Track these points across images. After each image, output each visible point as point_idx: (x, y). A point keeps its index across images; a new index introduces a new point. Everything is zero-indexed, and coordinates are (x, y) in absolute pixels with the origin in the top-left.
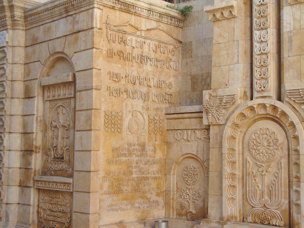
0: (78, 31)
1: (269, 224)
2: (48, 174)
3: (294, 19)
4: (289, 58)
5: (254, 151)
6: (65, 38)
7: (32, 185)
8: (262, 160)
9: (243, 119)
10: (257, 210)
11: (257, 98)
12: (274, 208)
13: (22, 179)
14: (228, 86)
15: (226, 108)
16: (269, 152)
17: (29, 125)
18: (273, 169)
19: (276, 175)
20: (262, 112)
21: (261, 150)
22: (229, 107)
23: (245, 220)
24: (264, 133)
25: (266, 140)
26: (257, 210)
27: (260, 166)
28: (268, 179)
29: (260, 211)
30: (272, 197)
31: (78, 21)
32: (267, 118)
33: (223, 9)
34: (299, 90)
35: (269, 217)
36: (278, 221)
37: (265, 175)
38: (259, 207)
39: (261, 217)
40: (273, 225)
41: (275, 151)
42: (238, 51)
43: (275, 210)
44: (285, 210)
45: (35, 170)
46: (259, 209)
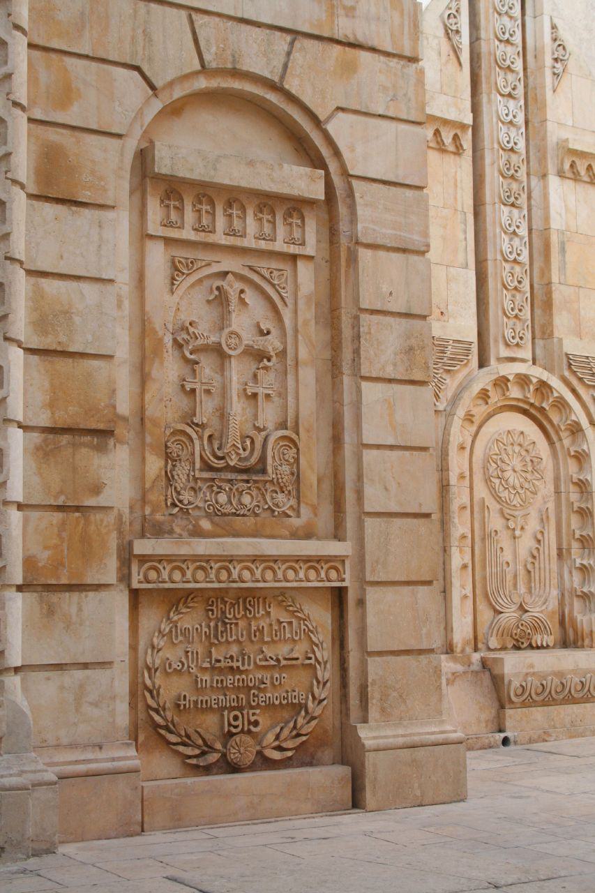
0: (352, 40)
1: (531, 647)
2: (177, 530)
3: (567, 209)
4: (562, 287)
5: (497, 481)
7: (111, 576)
8: (515, 502)
9: (477, 405)
10: (508, 619)
11: (499, 360)
12: (538, 609)
13: (44, 556)
14: (445, 318)
15: (449, 370)
16: (526, 485)
17: (77, 319)
18: (533, 525)
19: (539, 537)
20: (515, 392)
21: (511, 480)
22: (457, 371)
23: (480, 645)
24: (516, 439)
25: (520, 459)
26: (508, 619)
27: (508, 517)
28: (526, 543)
29: (512, 620)
30: (533, 585)
32: (525, 412)
33: (446, 122)
34: (587, 357)
35: (529, 631)
36: (545, 636)
37: (520, 537)
38: (512, 610)
39: (516, 634)
40: (538, 648)
41: (536, 482)
42: (466, 238)
43: (541, 615)
44: (553, 613)
45: (120, 516)
46: (510, 615)
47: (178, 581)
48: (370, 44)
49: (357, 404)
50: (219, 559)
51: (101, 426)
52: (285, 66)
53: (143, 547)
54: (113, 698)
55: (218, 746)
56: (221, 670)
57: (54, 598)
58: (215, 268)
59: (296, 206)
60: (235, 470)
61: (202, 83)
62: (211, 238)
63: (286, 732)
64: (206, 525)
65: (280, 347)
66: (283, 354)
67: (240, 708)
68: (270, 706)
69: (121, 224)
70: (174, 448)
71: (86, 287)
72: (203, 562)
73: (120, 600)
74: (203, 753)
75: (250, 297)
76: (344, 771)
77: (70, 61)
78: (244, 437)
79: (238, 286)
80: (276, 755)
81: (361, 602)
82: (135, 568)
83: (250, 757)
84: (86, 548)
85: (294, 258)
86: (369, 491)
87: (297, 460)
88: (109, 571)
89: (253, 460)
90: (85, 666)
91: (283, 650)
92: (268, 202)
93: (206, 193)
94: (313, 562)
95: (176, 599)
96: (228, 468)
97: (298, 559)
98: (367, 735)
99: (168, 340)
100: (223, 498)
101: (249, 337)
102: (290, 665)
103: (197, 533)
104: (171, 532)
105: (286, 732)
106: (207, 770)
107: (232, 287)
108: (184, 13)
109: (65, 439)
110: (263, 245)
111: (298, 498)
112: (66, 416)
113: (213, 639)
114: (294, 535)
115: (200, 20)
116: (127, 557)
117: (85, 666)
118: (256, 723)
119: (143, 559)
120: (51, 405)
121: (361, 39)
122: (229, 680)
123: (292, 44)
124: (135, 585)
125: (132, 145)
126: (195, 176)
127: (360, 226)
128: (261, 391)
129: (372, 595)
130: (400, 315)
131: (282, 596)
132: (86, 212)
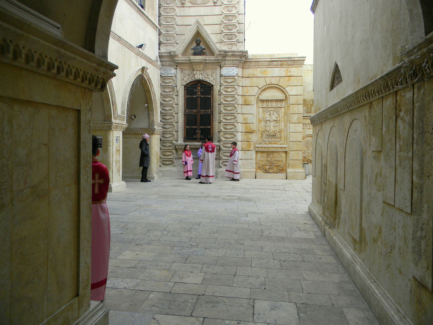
0: (290, 76)
2: (263, 143)
6: (279, 78)
17: (248, 119)
31: (291, 71)
47: (261, 150)
48: (293, 76)
49: (289, 127)
50: (268, 147)
51: (252, 131)
52: (279, 82)
53: (257, 146)
54: (253, 163)
55: (268, 170)
56: (268, 161)
57: (246, 151)
58: (269, 110)
59: (281, 101)
60: (272, 136)
61: (267, 86)
62: (268, 106)
63: (278, 169)
64: (267, 143)
65: (279, 119)
66: (279, 120)
67: (271, 166)
68: (275, 166)
69: (255, 106)
70: (263, 133)
71: (250, 115)
72: (265, 147)
73: (254, 153)
74: (266, 171)
75: (275, 113)
76: (285, 174)
77: (248, 87)
78: (273, 131)
79: (273, 112)
80: (276, 172)
81: (289, 153)
82: (256, 148)
83: (272, 172)
84: (249, 146)
85: (281, 107)
86: (290, 138)
87: (281, 134)
88: (252, 148)
89: (274, 135)
90: (250, 159)
91: (277, 159)
92: (277, 101)
93: (267, 101)
94: (281, 148)
95: (262, 152)
96: (271, 136)
97: (279, 147)
98: (288, 170)
99: (262, 120)
100: (270, 139)
101: (274, 119)
102: (279, 161)
103: (266, 144)
104: (262, 144)
105: (278, 169)
106: (266, 173)
107: (272, 112)
108: (264, 78)
109: (247, 133)
110: (276, 106)
111: (281, 139)
112: (247, 131)
113: (267, 157)
114: (281, 144)
115: (266, 78)
116: (255, 147)
117: (250, 159)
118: (273, 168)
119: (257, 147)
120: (246, 129)
121: (292, 75)
122: (270, 162)
123: (280, 78)
124: (256, 150)
125: (257, 96)
126: (265, 99)
127: (290, 102)
128: (276, 126)
129: (290, 152)
130: (297, 114)
131: (277, 152)
132: (250, 106)
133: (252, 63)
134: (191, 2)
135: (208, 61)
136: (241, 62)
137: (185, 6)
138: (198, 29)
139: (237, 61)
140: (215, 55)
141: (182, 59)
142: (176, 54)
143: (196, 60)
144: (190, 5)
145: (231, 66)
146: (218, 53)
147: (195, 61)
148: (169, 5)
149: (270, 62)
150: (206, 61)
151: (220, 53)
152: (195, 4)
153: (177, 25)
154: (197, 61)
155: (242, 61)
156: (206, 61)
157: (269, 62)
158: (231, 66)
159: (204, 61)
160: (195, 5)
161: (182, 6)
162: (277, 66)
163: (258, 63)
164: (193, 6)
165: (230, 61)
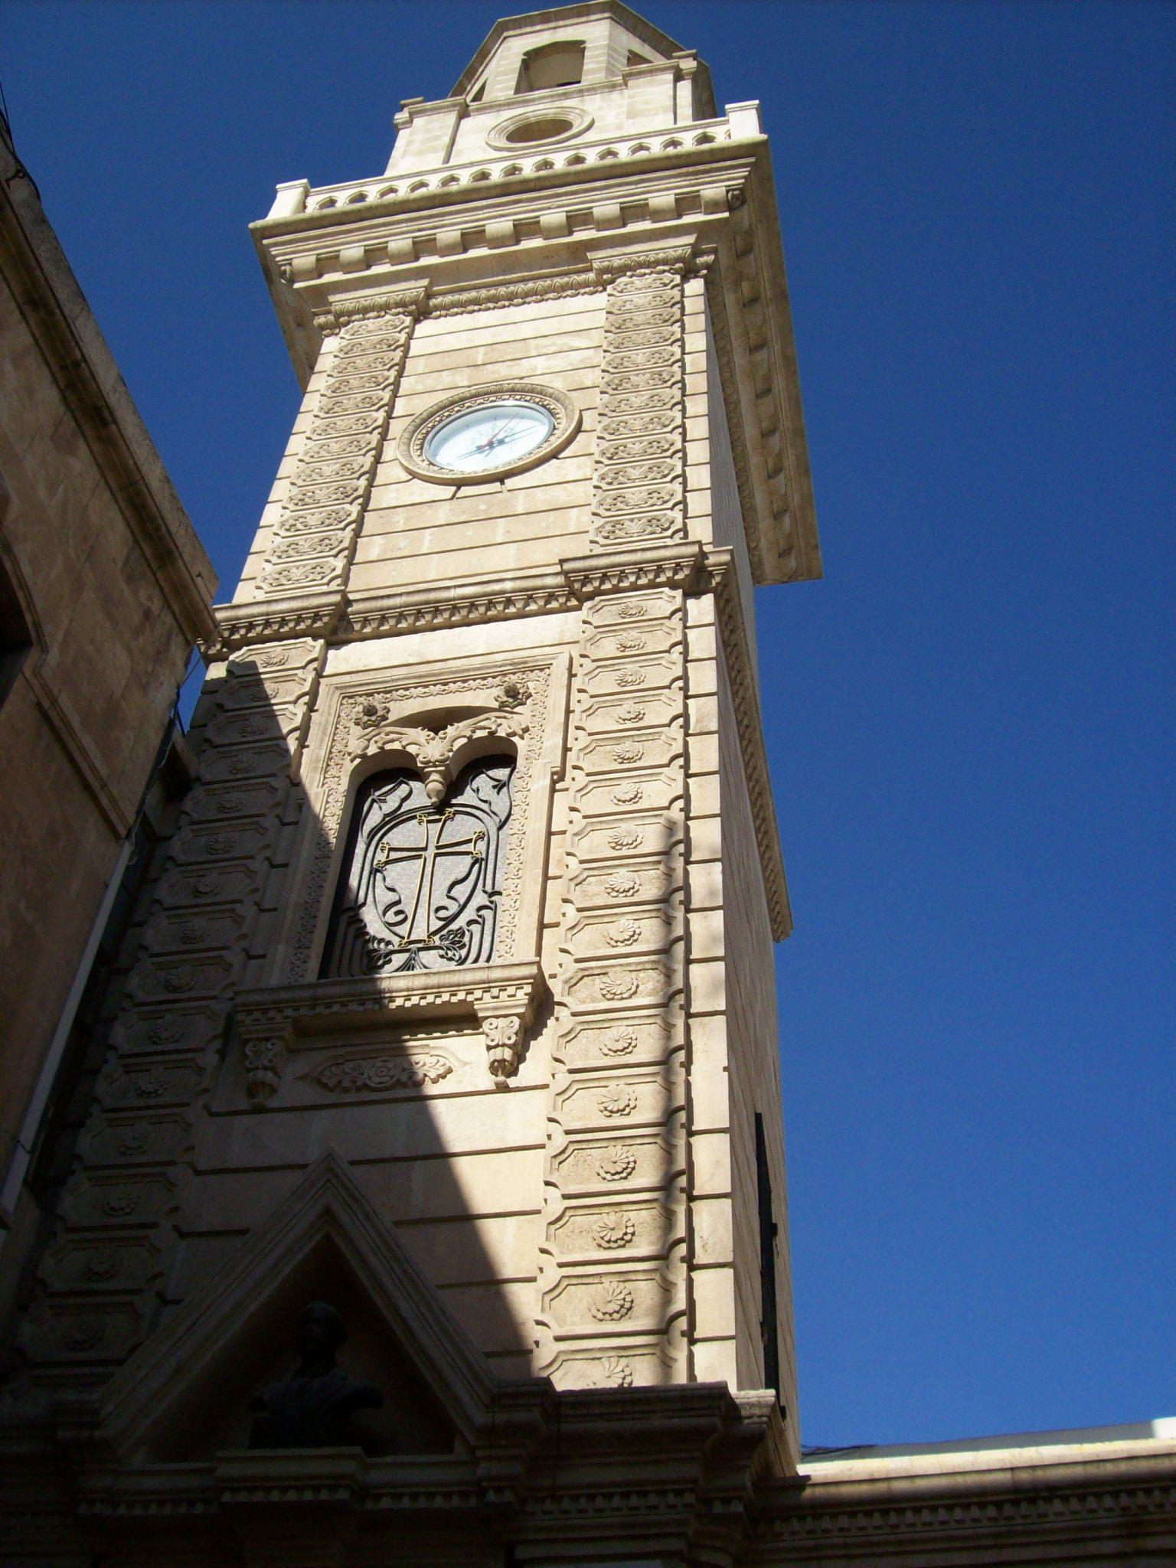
133: (826, 1523)
134: (319, 1082)
135: (386, 1503)
136: (718, 1508)
137: (273, 1102)
138: (328, 1238)
139: (671, 1498)
140: (458, 1446)
141: (148, 1483)
142: (98, 1433)
143: (268, 1490)
144: (310, 1094)
145: (620, 1547)
146: (480, 1418)
147: (259, 1496)
148: (152, 1102)
149: (1008, 1509)
150: (369, 1505)
151: (501, 1418)
152: (346, 1090)
153: (176, 1228)
154: (275, 1496)
155: (727, 1501)
156: (369, 1505)
157: (999, 1505)
158: (620, 1547)
159: (343, 1495)
160: (353, 1097)
161: (243, 1104)
162: (1092, 1548)
163: (893, 1518)
164: (327, 1101)
165: (600, 1502)
